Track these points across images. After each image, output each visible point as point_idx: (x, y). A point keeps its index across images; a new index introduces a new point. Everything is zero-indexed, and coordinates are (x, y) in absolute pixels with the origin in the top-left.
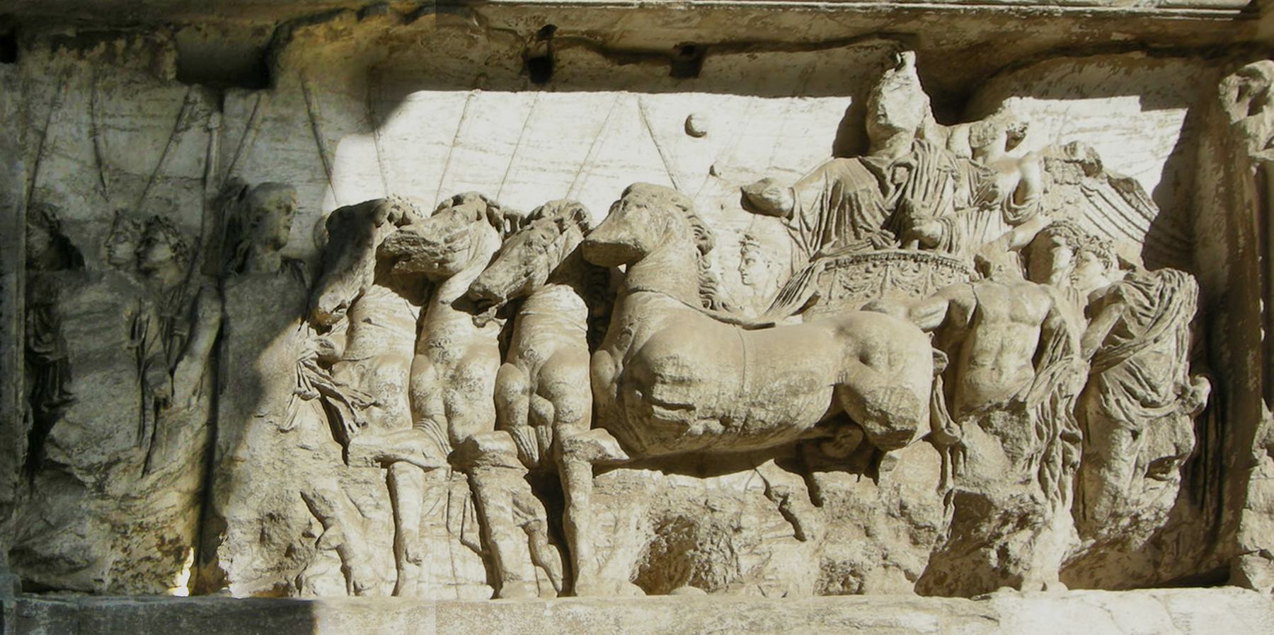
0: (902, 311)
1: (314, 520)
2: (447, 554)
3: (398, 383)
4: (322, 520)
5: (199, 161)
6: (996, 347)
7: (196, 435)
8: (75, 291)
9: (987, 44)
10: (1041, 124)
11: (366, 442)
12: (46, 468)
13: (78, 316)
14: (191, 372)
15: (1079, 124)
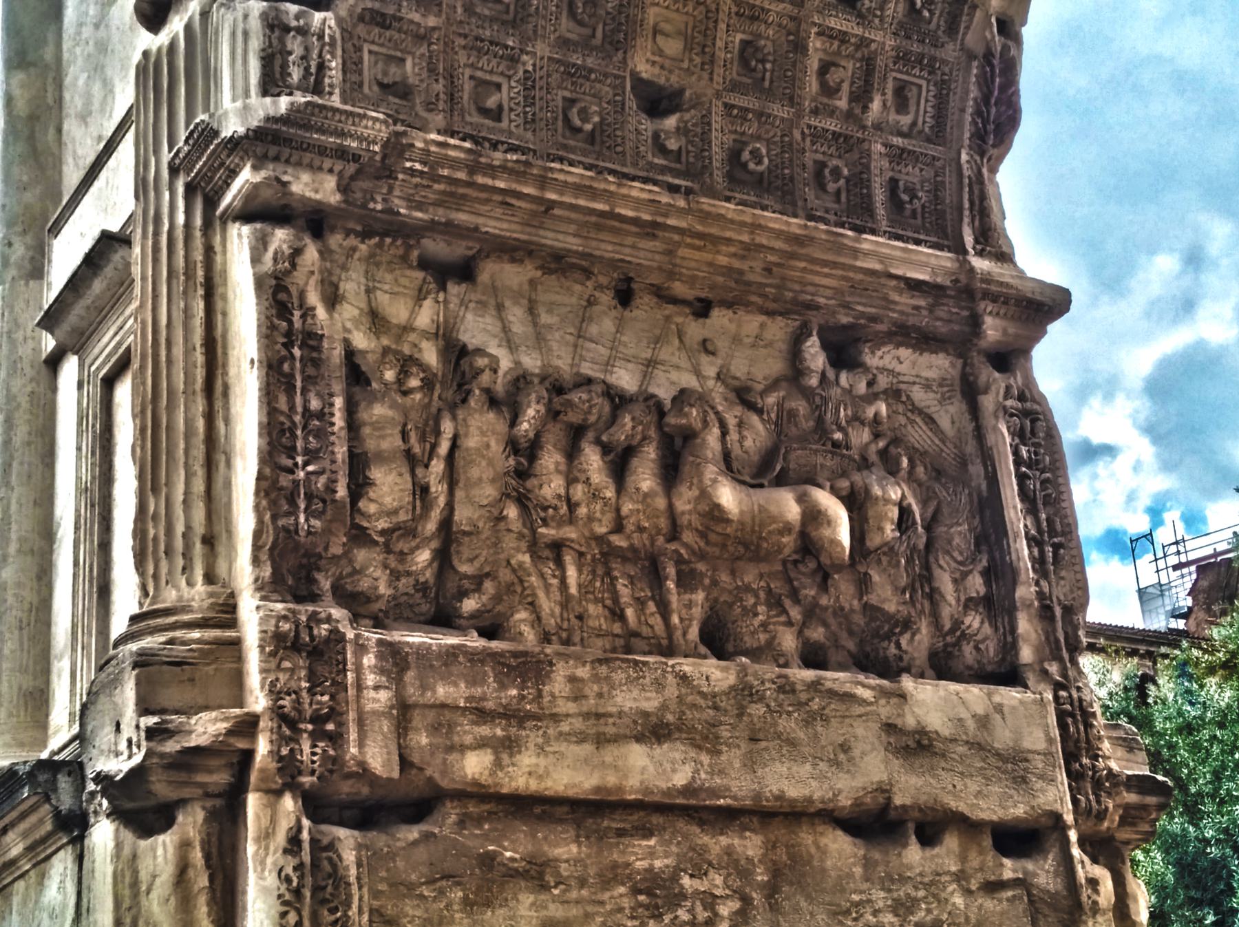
0: (828, 484)
5: (433, 321)
8: (370, 404)
14: (438, 466)
15: (901, 378)
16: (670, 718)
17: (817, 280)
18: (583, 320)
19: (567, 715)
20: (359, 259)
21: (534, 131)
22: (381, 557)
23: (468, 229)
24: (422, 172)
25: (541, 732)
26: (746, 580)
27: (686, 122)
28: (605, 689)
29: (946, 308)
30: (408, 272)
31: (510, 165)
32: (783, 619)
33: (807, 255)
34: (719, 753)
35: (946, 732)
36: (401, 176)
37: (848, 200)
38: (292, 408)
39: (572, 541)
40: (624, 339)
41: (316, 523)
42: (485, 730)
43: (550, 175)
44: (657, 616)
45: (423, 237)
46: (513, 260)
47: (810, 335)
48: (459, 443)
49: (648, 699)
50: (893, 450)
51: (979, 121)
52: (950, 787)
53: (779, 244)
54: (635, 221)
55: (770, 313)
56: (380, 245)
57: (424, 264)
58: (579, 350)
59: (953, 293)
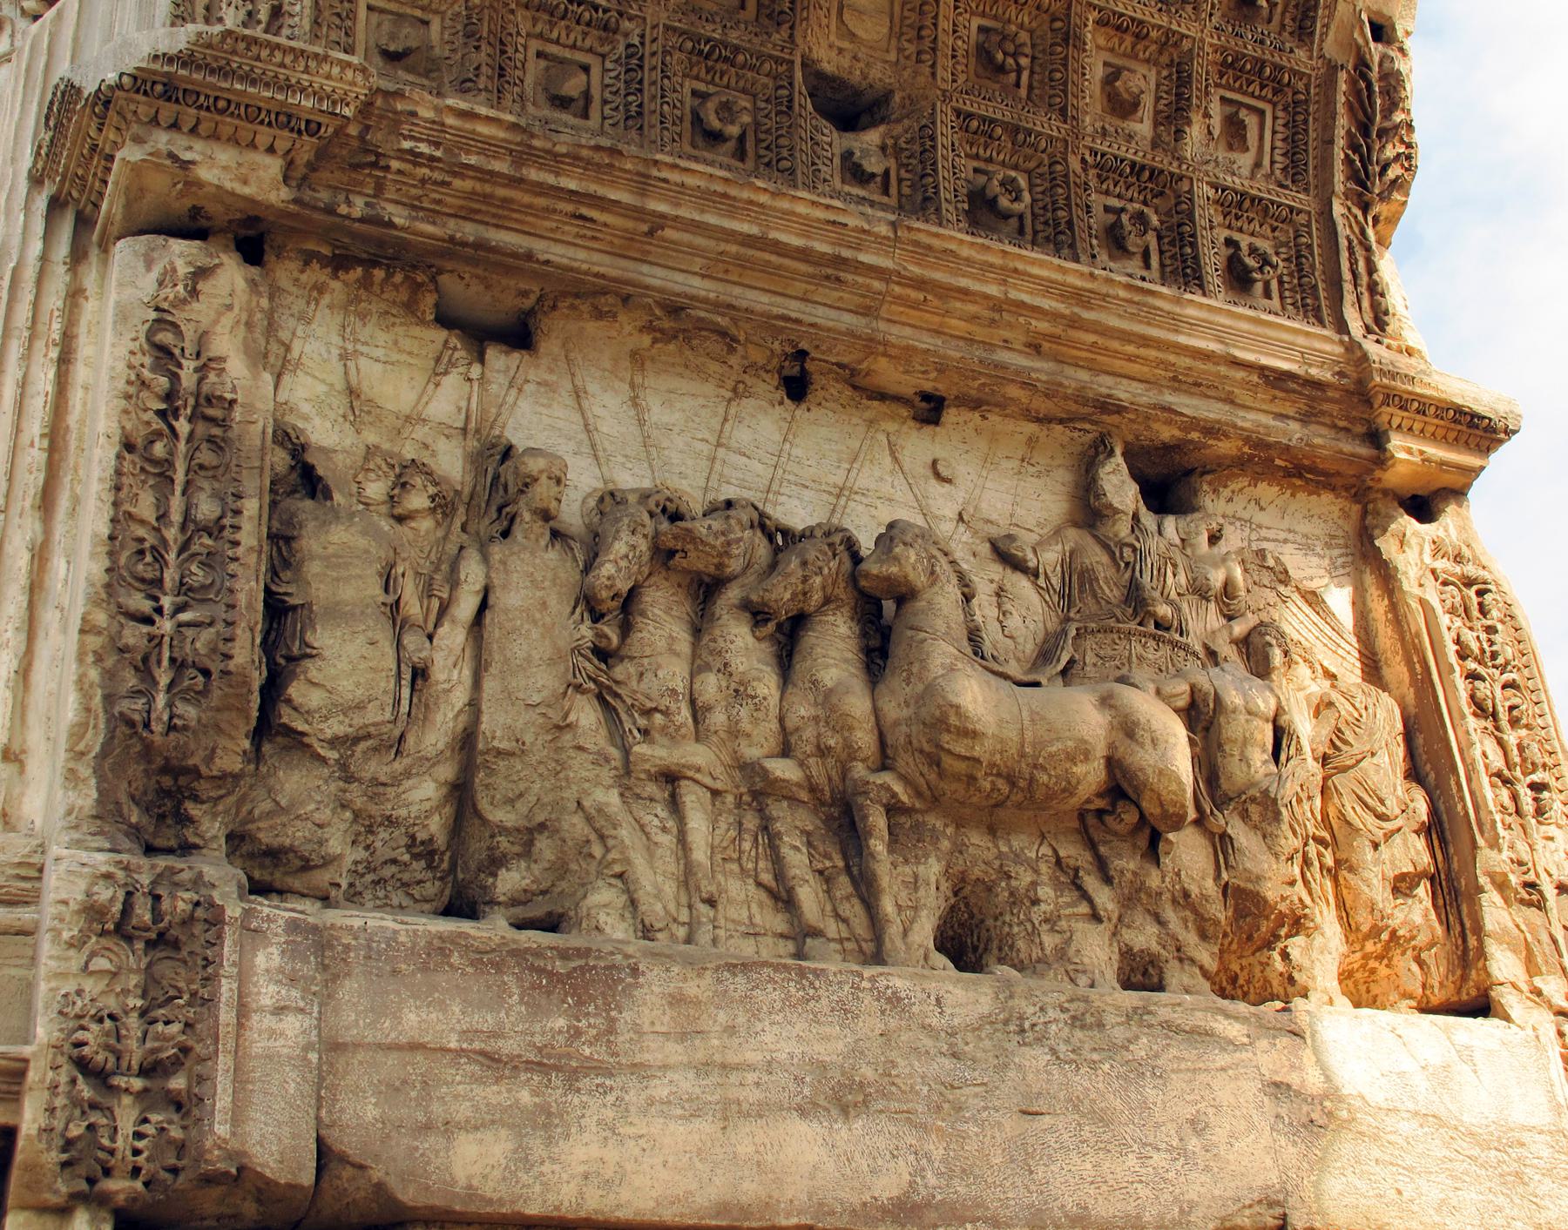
0: (1152, 687)
1: (593, 837)
3: (680, 690)
4: (602, 838)
5: (459, 409)
6: (1240, 739)
7: (456, 716)
9: (1178, 446)
11: (649, 752)
12: (278, 733)
13: (326, 558)
15: (1264, 533)
16: (868, 1072)
17: (1118, 364)
18: (726, 420)
19: (665, 1067)
20: (330, 307)
21: (641, 128)
22: (333, 787)
23: (515, 255)
24: (432, 158)
25: (610, 1098)
26: (1016, 844)
27: (896, 139)
28: (741, 1020)
29: (1327, 420)
30: (417, 331)
31: (585, 153)
32: (1084, 908)
33: (1096, 322)
34: (964, 1137)
35: (1377, 1097)
36: (395, 164)
37: (1162, 265)
38: (163, 517)
39: (699, 770)
40: (795, 452)
41: (189, 712)
42: (494, 1094)
43: (655, 173)
44: (855, 901)
45: (440, 272)
46: (599, 315)
47: (1111, 453)
48: (491, 601)
49: (826, 1038)
50: (1255, 639)
51: (1356, 158)
52: (1392, 1194)
53: (1047, 304)
54: (804, 255)
55: (1044, 420)
56: (366, 283)
57: (444, 320)
58: (718, 466)
59: (1337, 395)
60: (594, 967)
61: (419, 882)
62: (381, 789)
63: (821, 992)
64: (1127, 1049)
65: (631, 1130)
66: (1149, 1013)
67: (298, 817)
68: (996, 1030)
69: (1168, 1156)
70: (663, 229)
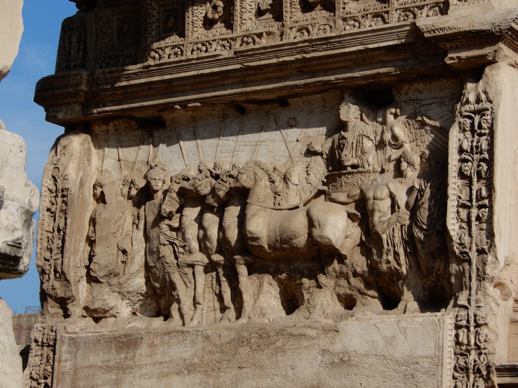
2: (212, 299)
10: (408, 105)
15: (422, 103)
16: (196, 360)
17: (332, 66)
20: (112, 134)
25: (132, 375)
26: (296, 265)
28: (166, 349)
39: (198, 261)
42: (106, 377)
56: (115, 125)
58: (219, 148)
60: (132, 339)
61: (152, 303)
62: (122, 285)
63: (188, 338)
64: (275, 344)
65: (136, 383)
66: (284, 331)
67: (97, 300)
68: (235, 343)
69: (281, 378)
70: (172, 82)
